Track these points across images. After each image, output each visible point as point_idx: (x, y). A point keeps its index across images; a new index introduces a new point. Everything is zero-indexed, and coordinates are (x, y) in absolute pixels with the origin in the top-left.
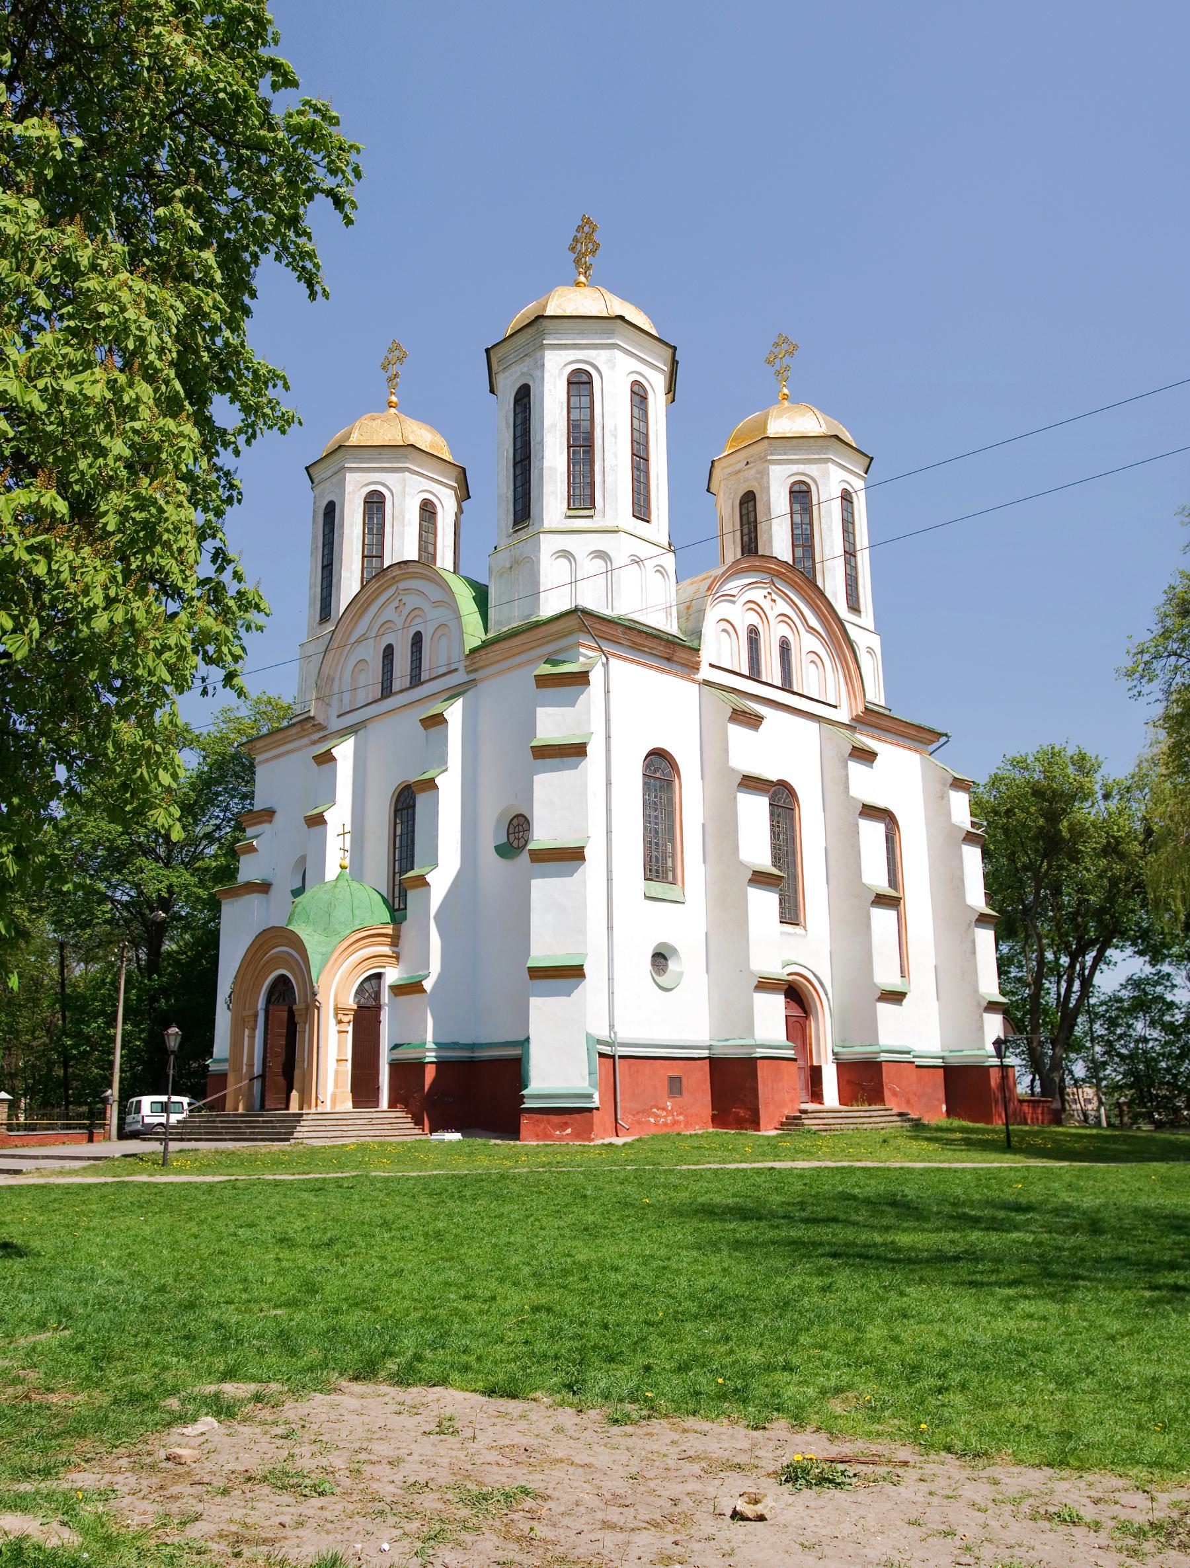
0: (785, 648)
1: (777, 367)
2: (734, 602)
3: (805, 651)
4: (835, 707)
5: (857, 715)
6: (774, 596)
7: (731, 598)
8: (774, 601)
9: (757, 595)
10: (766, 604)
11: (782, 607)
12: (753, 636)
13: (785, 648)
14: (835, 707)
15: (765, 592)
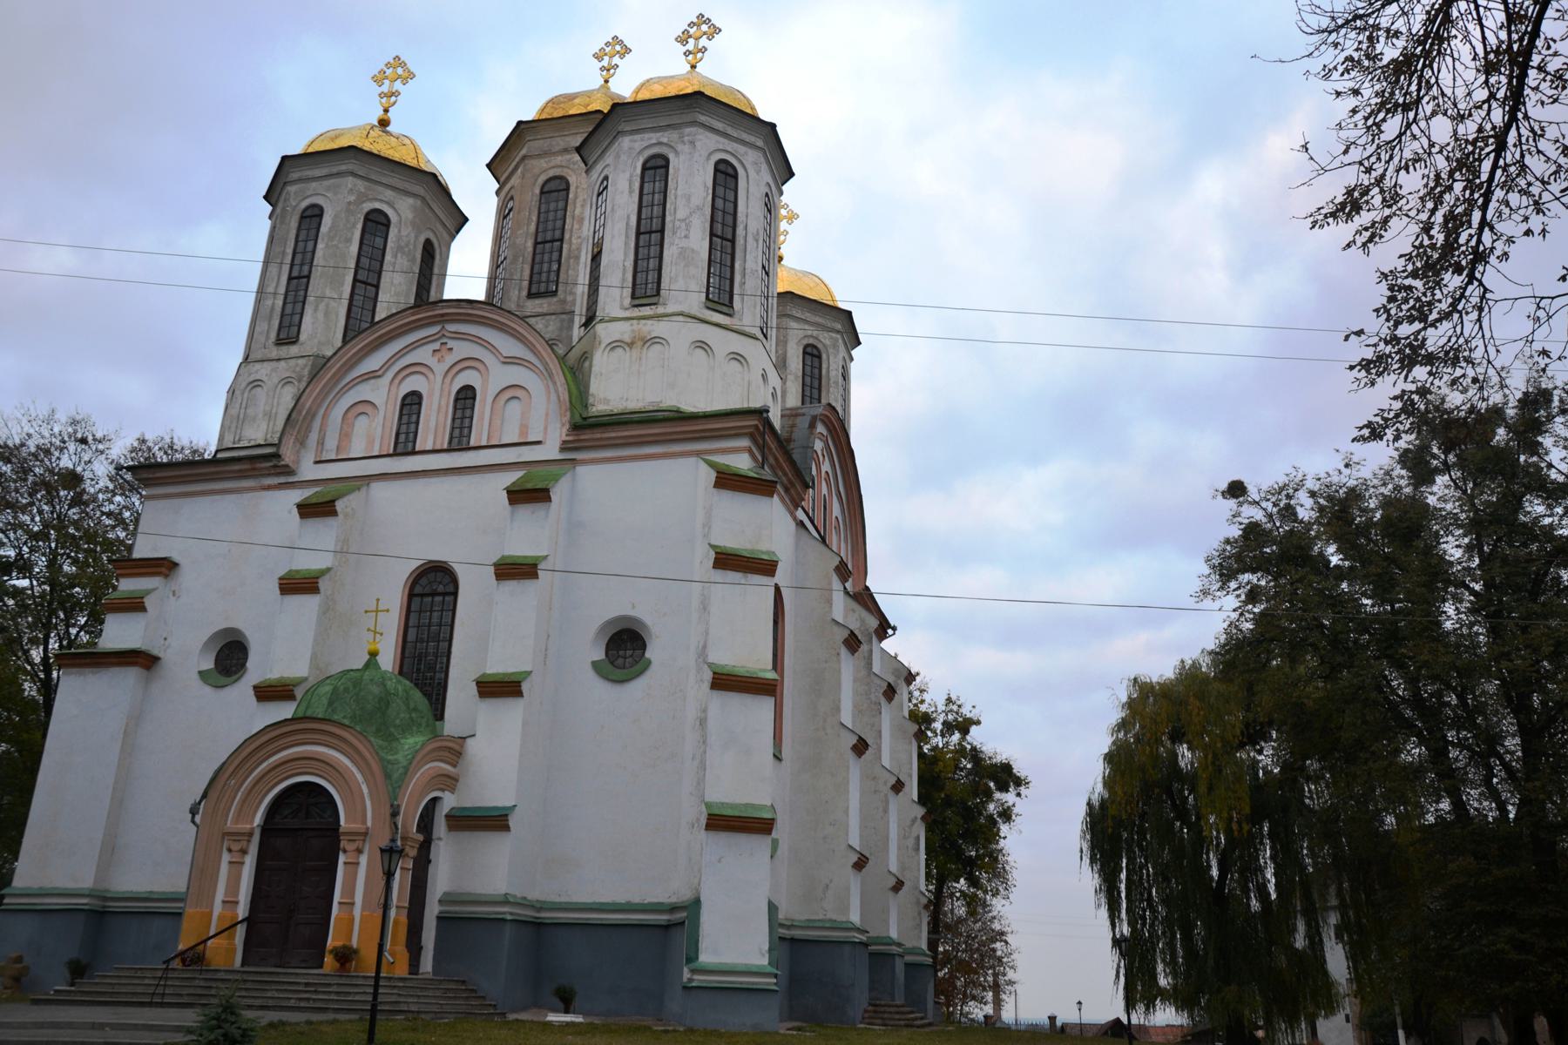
0: (466, 396)
1: (691, 45)
2: (379, 376)
3: (493, 389)
4: (539, 443)
5: (564, 442)
6: (451, 344)
7: (373, 375)
8: (451, 349)
9: (423, 355)
10: (431, 361)
11: (462, 349)
12: (412, 402)
13: (466, 396)
14: (539, 443)
15: (437, 346)
